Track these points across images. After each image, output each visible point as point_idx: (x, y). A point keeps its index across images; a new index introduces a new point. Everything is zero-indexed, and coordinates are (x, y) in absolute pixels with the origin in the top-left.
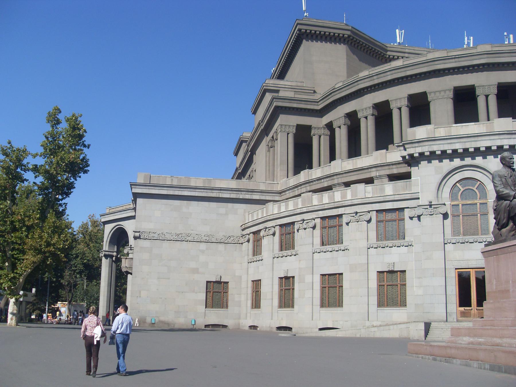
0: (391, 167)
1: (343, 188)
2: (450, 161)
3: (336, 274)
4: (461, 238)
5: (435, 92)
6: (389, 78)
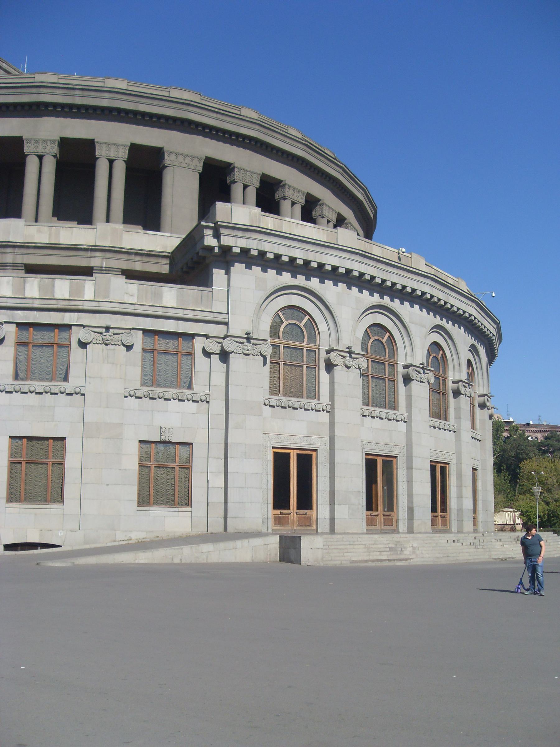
0: (133, 257)
1: (22, 273)
2: (278, 274)
3: (47, 439)
4: (280, 399)
5: (177, 154)
6: (105, 103)
